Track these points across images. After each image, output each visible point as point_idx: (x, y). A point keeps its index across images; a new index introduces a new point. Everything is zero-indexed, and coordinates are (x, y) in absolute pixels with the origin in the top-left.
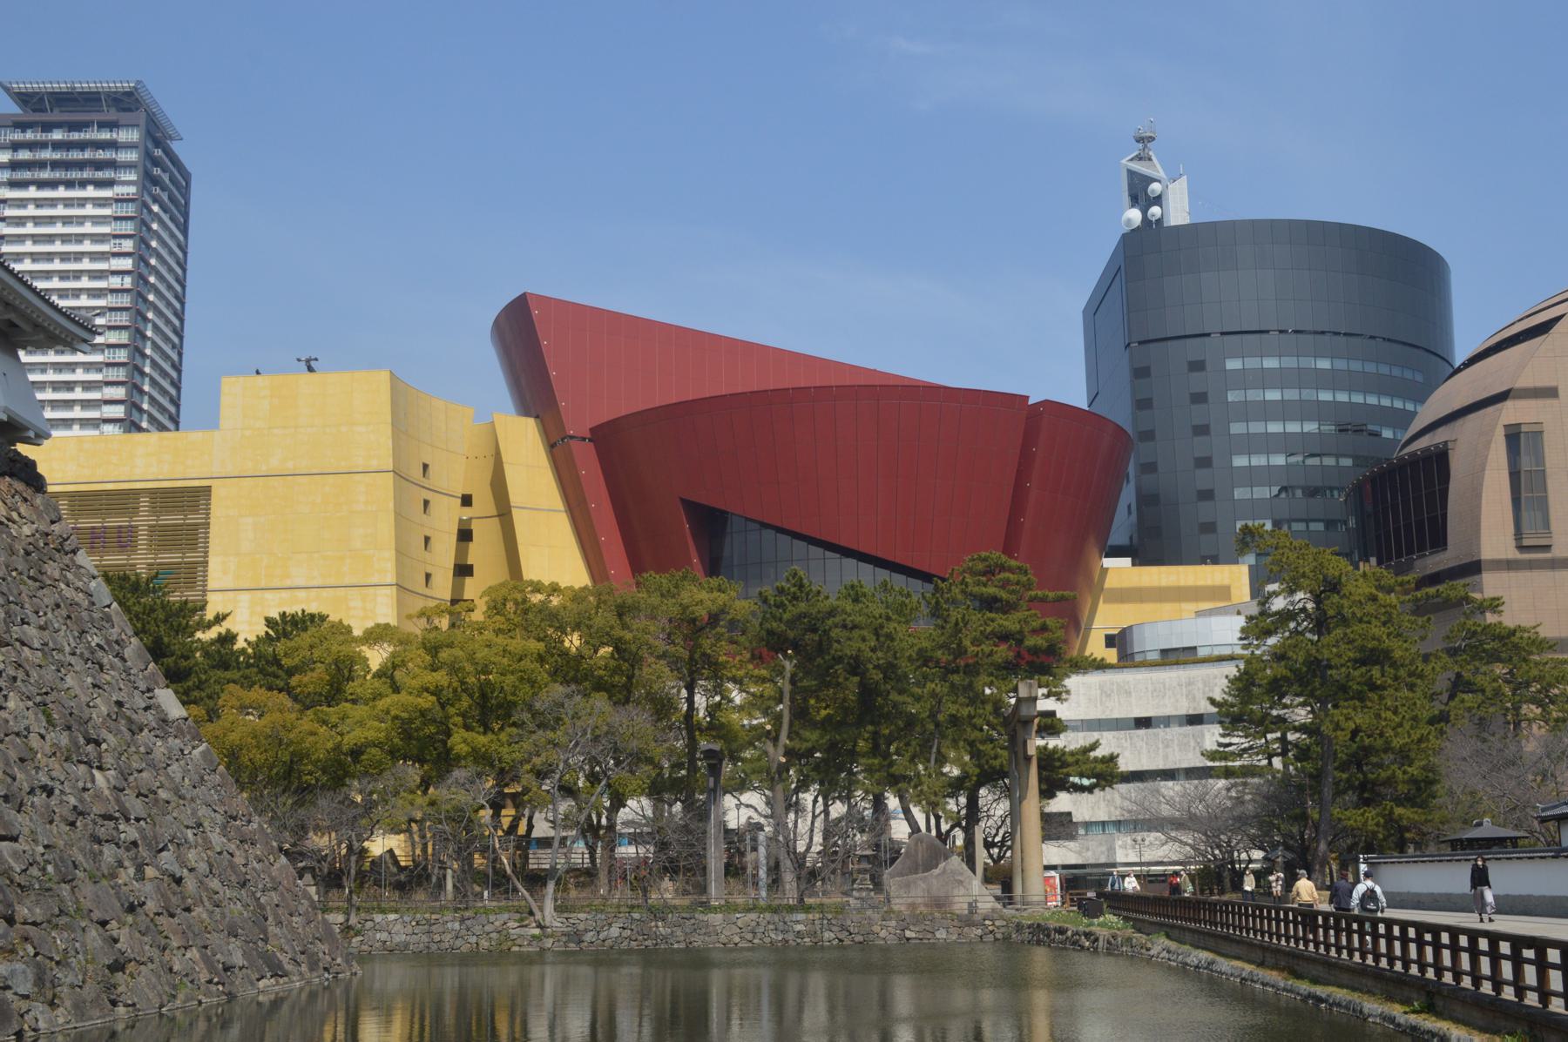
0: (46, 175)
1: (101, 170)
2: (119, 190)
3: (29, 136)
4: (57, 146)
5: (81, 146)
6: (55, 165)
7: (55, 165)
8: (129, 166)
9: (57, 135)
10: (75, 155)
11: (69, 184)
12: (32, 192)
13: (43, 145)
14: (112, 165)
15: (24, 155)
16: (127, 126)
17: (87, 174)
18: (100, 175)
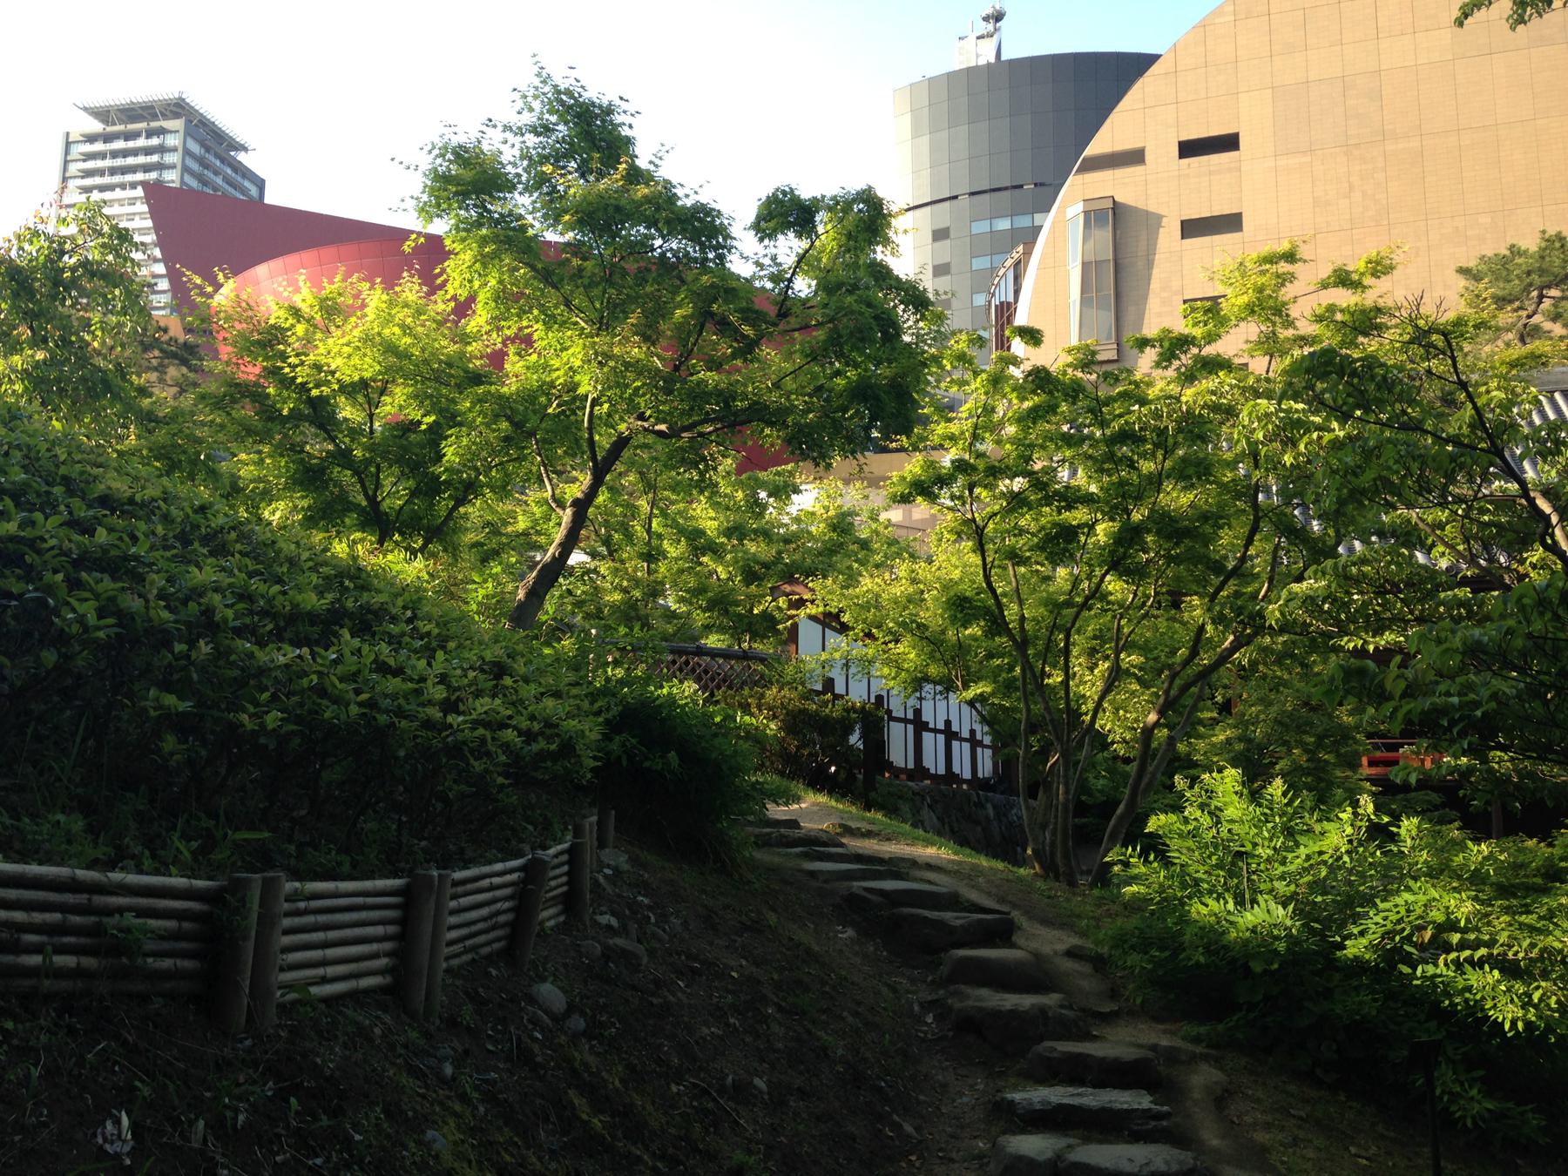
4: (115, 154)
5: (135, 152)
6: (113, 171)
7: (113, 171)
10: (131, 161)
11: (123, 186)
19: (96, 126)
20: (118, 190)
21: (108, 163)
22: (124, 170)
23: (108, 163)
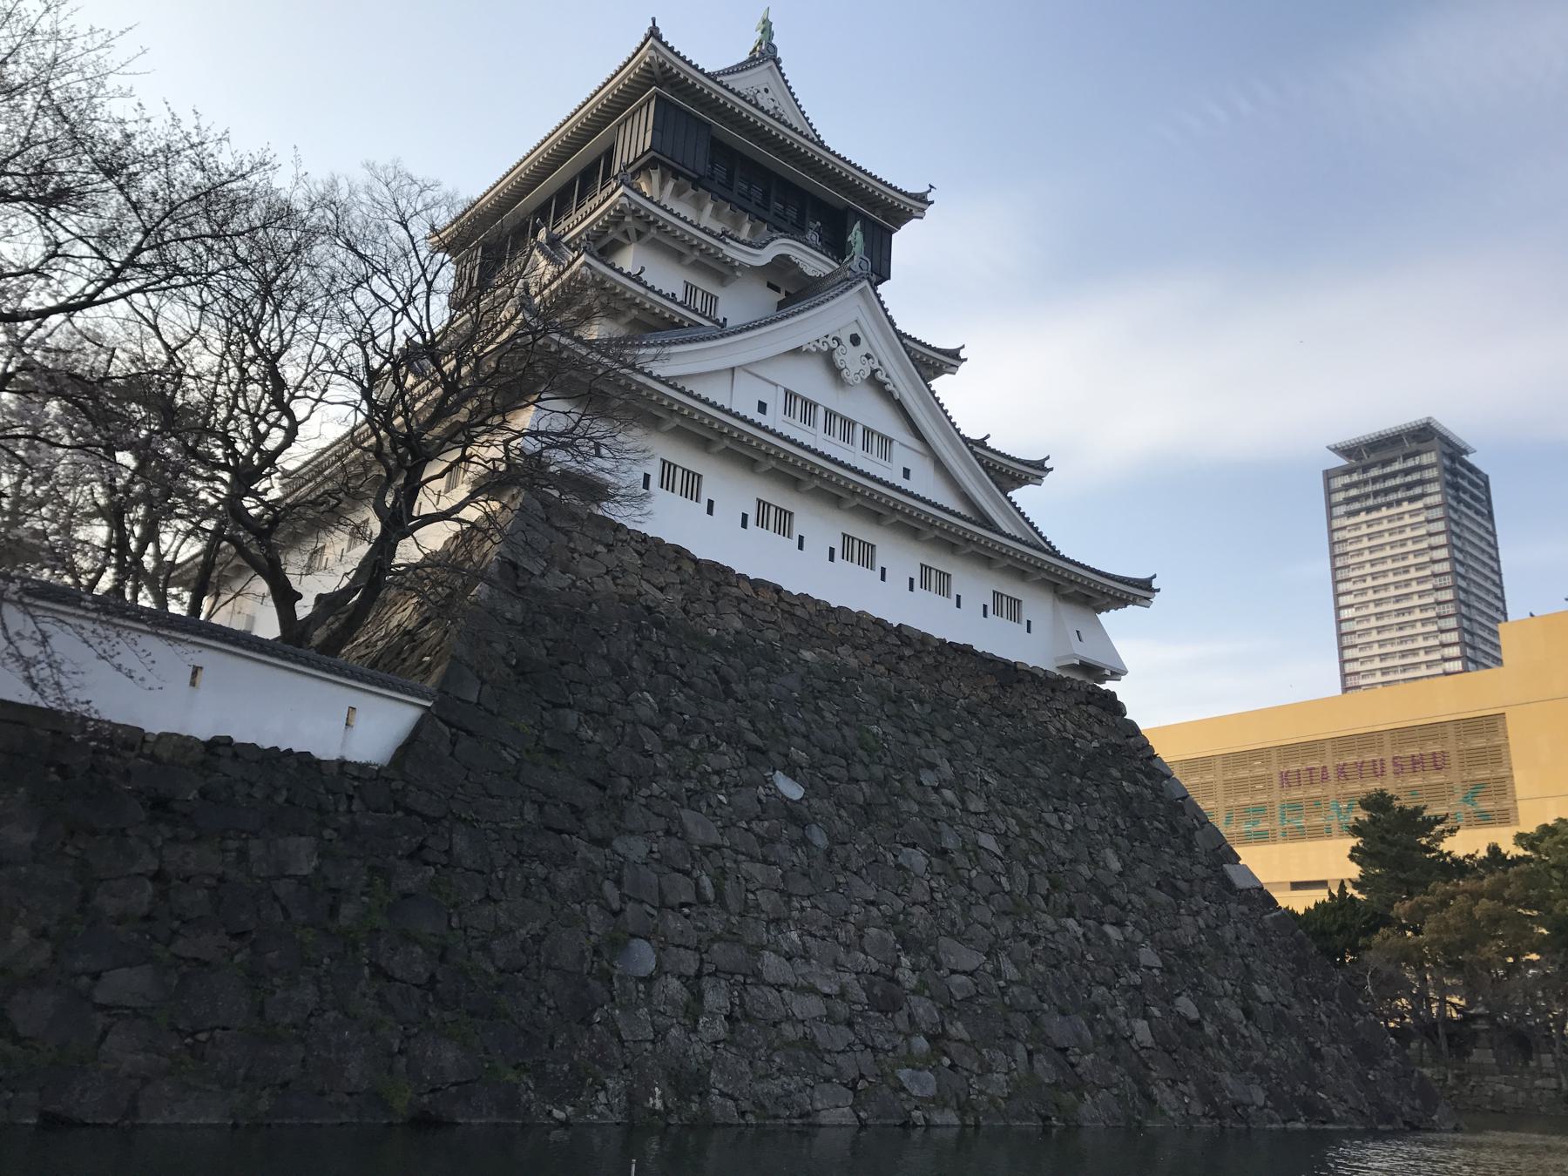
0: (1371, 502)
1: (1412, 489)
2: (1429, 500)
3: (1355, 477)
4: (1375, 480)
5: (1394, 475)
6: (1376, 494)
7: (1376, 494)
8: (1430, 481)
9: (1375, 472)
11: (1389, 505)
12: (1363, 517)
13: (1365, 482)
14: (1421, 482)
15: (1353, 492)
16: (1426, 452)
17: (1400, 495)
18: (1411, 493)
19: (1342, 462)
20: (1384, 509)
21: (1370, 488)
22: (1386, 492)
23: (1370, 488)
